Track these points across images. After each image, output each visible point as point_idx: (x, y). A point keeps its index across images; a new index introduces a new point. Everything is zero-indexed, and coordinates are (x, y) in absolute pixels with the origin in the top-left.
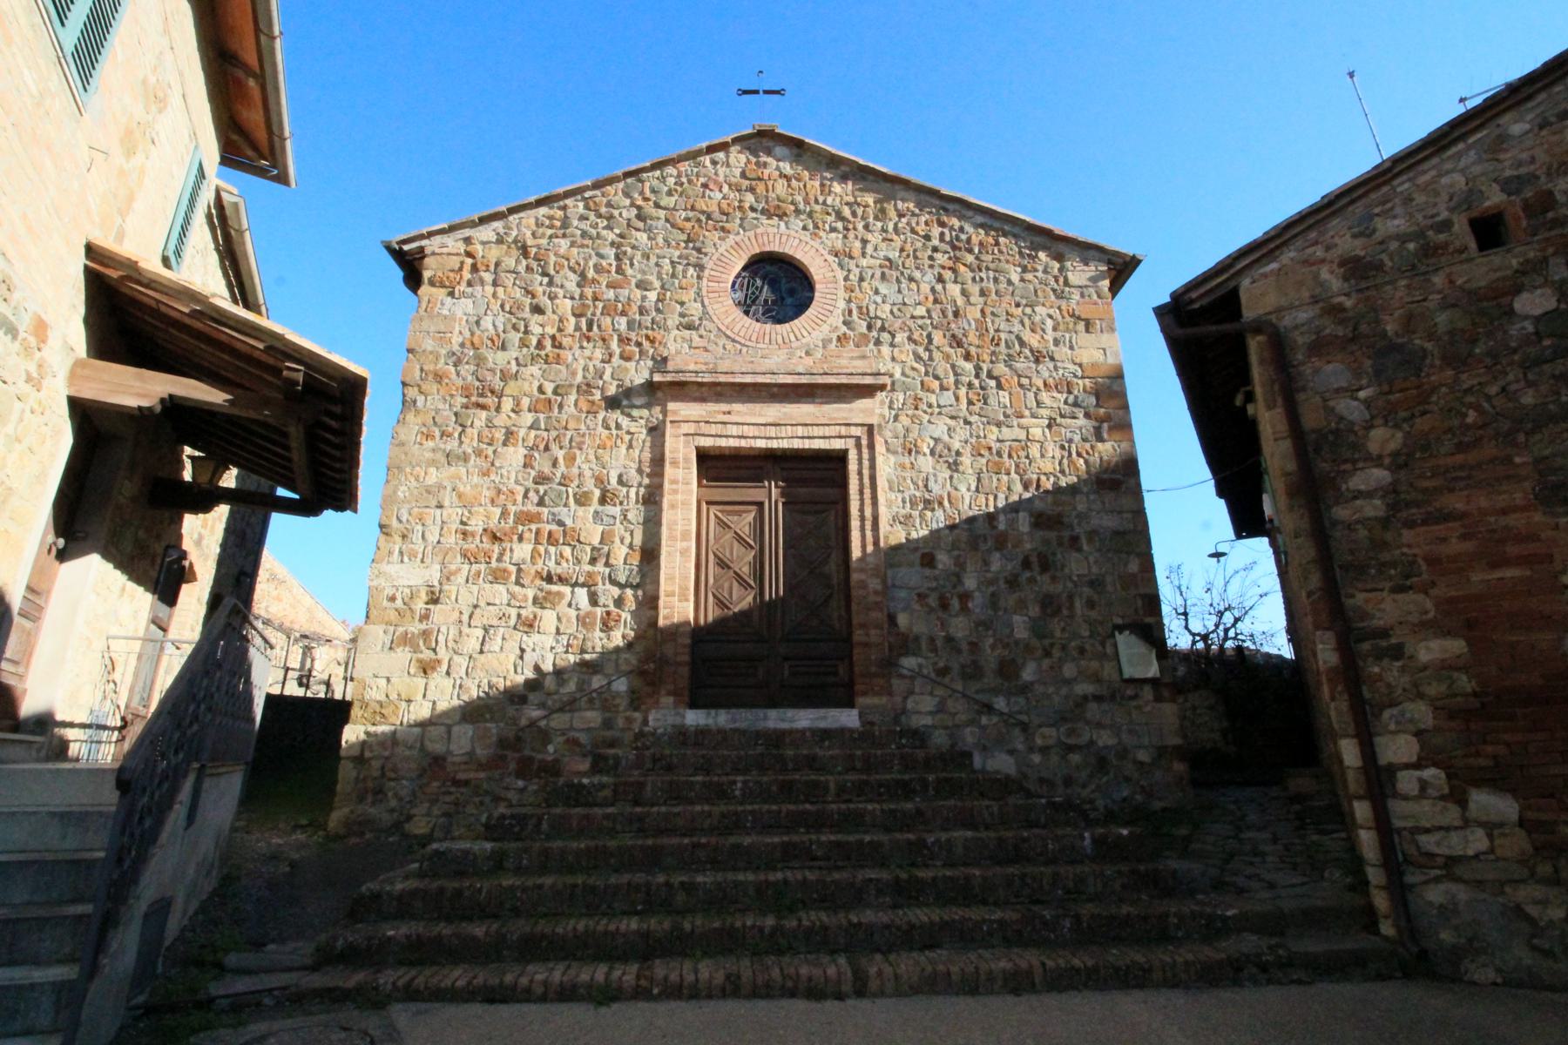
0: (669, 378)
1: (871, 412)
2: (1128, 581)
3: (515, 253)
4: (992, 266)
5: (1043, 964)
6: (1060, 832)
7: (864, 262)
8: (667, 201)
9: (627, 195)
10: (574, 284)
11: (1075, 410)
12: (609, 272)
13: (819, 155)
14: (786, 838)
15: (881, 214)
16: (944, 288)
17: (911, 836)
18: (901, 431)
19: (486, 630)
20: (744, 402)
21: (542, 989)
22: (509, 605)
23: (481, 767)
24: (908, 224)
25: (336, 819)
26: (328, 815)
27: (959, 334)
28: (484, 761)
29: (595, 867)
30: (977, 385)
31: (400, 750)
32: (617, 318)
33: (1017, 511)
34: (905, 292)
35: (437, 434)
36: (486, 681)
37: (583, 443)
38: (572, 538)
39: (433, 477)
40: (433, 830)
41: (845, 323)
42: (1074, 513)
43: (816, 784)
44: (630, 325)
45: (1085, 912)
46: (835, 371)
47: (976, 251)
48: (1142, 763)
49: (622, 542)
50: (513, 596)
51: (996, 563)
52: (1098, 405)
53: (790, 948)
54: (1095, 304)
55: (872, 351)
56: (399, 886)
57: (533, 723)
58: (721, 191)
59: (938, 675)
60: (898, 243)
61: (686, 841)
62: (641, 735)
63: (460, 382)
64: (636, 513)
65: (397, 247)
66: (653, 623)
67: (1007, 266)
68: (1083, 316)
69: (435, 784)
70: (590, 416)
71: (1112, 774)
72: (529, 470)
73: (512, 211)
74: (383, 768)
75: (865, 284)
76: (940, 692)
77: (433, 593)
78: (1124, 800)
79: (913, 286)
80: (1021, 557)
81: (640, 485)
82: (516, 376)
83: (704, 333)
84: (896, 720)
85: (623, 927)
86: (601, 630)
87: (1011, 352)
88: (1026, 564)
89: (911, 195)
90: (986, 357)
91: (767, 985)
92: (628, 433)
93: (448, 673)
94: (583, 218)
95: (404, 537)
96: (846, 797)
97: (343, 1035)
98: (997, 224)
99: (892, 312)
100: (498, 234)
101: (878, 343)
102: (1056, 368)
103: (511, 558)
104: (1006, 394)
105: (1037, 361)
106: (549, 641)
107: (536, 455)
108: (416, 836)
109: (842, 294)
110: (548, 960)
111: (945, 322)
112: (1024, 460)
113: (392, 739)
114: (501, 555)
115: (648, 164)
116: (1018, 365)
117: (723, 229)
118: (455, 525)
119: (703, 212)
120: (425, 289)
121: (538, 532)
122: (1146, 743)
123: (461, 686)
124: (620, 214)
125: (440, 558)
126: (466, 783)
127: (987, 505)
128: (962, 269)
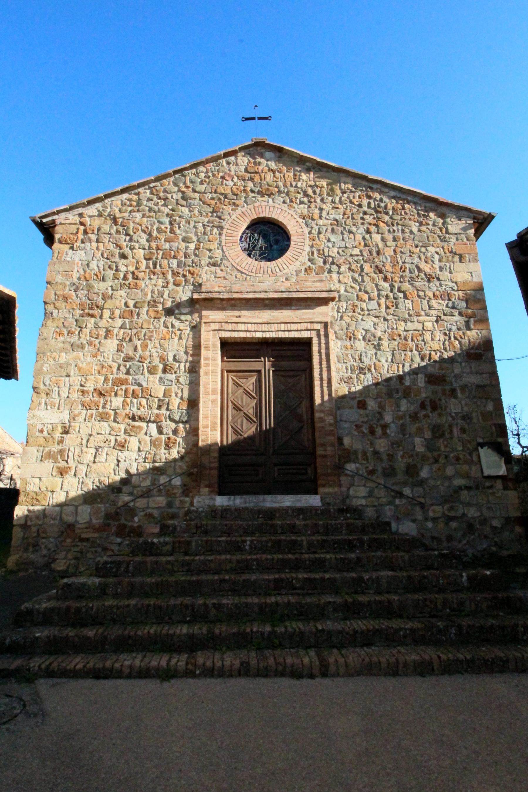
0: (203, 296)
1: (326, 315)
2: (486, 416)
3: (109, 222)
4: (400, 222)
5: (439, 657)
6: (447, 573)
7: (321, 222)
8: (200, 188)
9: (175, 184)
10: (145, 240)
11: (453, 311)
12: (166, 232)
13: (292, 156)
14: (277, 576)
15: (331, 192)
16: (371, 237)
17: (353, 575)
18: (345, 326)
19: (96, 449)
20: (248, 310)
21: (129, 671)
22: (110, 434)
23: (97, 530)
24: (348, 197)
25: (11, 561)
26: (7, 558)
27: (380, 265)
28: (97, 526)
29: (162, 593)
30: (392, 297)
31: (47, 520)
32: (171, 260)
33: (417, 374)
34: (347, 240)
35: (66, 333)
36: (97, 480)
37: (152, 336)
38: (147, 394)
39: (64, 358)
40: (68, 567)
41: (309, 260)
42: (453, 375)
43: (294, 542)
44: (179, 265)
45: (464, 623)
46: (304, 290)
47: (391, 213)
48: (495, 528)
49: (176, 395)
50: (112, 428)
51: (404, 405)
52: (467, 308)
53: (280, 645)
54: (466, 244)
55: (326, 277)
56: (44, 605)
57: (126, 504)
58: (232, 181)
59: (368, 474)
60: (342, 209)
61: (216, 577)
62: (189, 512)
63: (78, 301)
64: (184, 378)
65: (39, 221)
66: (196, 444)
67: (410, 222)
68: (458, 252)
69: (69, 540)
70: (156, 320)
71: (476, 534)
72: (120, 353)
73: (107, 196)
74: (38, 531)
75: (321, 236)
76: (370, 484)
77: (65, 427)
78: (485, 550)
79: (352, 236)
80: (419, 402)
81: (186, 361)
82: (111, 297)
83: (224, 268)
84: (344, 501)
85: (178, 631)
86: (165, 449)
87: (413, 275)
88: (423, 406)
89: (348, 180)
90: (397, 279)
91: (266, 668)
92: (179, 330)
93: (75, 475)
94: (149, 200)
95: (47, 394)
96: (313, 550)
97: (7, 700)
98: (403, 196)
99: (338, 253)
100: (99, 211)
101: (330, 272)
102: (441, 285)
103: (111, 406)
104: (410, 302)
105: (429, 281)
106: (134, 455)
107: (124, 344)
108: (59, 571)
109: (307, 242)
110: (133, 651)
111: (371, 258)
112: (421, 342)
113: (43, 514)
114: (105, 404)
115: (188, 165)
116: (417, 284)
117: (234, 204)
118: (78, 387)
119: (222, 194)
120: (56, 245)
121: (126, 391)
122: (498, 514)
123: (83, 483)
124: (172, 197)
125: (69, 406)
126: (87, 540)
127: (398, 370)
128: (382, 225)
